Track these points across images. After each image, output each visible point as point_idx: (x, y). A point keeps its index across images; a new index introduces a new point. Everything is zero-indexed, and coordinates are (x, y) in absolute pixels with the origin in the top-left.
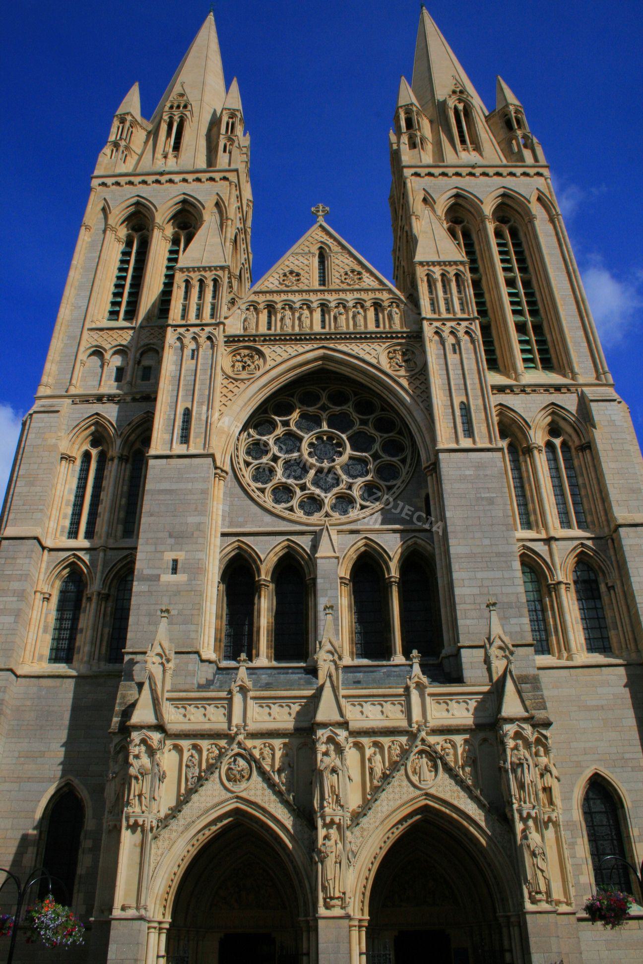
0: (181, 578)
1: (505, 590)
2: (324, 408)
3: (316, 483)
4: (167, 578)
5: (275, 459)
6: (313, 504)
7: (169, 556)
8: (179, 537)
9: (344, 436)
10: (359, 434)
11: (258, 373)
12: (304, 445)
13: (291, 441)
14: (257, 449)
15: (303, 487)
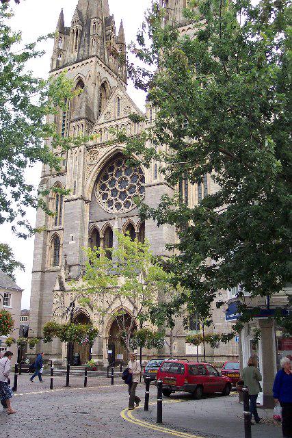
0: (74, 242)
1: (160, 237)
2: (123, 166)
3: (120, 197)
4: (71, 242)
5: (108, 190)
6: (118, 206)
7: (71, 235)
8: (73, 229)
9: (128, 178)
10: (134, 175)
11: (98, 160)
12: (117, 183)
13: (112, 182)
14: (103, 187)
15: (116, 200)
